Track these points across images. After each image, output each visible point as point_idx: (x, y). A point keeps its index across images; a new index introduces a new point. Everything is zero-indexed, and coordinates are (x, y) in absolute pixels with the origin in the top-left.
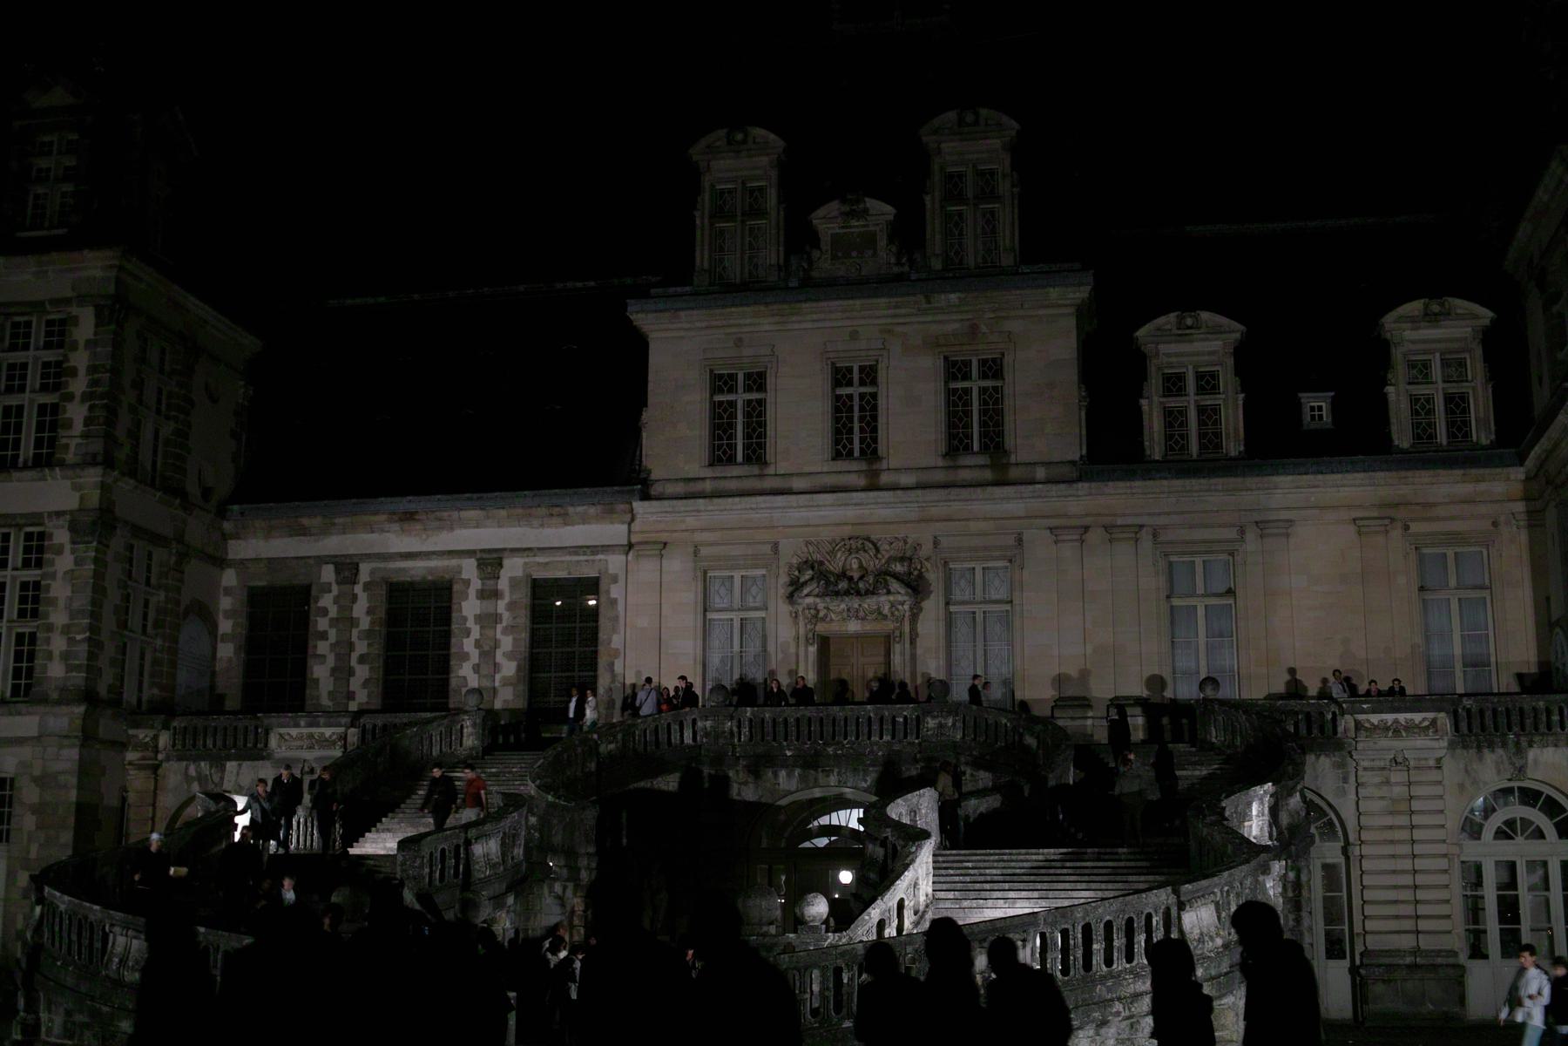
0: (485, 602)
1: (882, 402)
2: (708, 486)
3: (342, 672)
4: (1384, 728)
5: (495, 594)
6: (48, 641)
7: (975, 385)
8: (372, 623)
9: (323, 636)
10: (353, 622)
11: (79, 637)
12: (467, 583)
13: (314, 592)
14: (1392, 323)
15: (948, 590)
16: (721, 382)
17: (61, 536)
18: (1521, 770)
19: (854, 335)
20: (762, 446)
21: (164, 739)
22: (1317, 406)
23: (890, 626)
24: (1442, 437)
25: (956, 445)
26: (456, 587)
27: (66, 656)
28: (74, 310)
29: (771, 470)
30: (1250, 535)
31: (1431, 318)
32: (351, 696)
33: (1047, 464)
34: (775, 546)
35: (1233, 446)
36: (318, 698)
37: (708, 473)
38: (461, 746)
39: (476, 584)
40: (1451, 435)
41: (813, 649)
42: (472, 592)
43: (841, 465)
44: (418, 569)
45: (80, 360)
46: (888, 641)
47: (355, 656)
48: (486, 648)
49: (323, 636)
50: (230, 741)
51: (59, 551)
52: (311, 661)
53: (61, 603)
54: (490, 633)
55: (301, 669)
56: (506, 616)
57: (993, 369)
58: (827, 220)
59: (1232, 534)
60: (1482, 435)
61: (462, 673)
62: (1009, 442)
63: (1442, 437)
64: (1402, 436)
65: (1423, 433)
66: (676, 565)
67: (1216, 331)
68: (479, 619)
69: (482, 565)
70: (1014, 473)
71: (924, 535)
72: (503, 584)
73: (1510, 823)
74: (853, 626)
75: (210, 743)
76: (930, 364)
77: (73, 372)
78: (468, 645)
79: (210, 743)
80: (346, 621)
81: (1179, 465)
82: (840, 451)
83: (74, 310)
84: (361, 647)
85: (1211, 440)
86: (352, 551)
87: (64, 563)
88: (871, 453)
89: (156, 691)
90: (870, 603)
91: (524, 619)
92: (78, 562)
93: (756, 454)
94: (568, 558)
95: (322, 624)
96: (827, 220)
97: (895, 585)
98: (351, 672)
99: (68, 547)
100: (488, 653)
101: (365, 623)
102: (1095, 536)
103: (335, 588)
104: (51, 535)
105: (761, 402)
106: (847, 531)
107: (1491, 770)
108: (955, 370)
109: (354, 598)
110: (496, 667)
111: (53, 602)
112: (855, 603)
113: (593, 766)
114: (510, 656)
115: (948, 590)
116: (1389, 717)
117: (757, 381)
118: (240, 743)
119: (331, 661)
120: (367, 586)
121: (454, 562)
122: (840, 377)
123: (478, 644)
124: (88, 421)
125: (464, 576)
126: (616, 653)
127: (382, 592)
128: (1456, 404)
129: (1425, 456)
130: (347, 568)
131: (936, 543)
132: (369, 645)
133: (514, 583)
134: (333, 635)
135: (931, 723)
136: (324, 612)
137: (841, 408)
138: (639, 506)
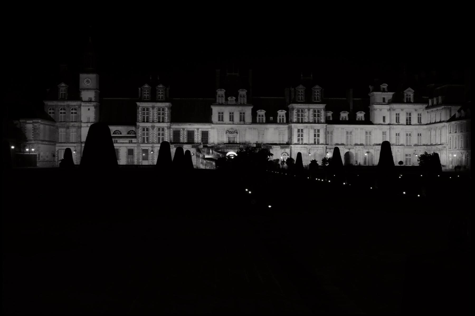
1: (234, 116)
2: (218, 123)
4: (275, 147)
7: (242, 115)
9: (181, 135)
10: (184, 134)
12: (196, 131)
13: (180, 131)
14: (278, 112)
15: (240, 132)
16: (219, 113)
17: (166, 129)
18: (285, 151)
19: (232, 110)
20: (223, 119)
21: (173, 146)
22: (271, 118)
23: (235, 136)
24: (282, 122)
25: (241, 120)
26: (195, 131)
27: (167, 139)
28: (165, 108)
29: (224, 122)
30: (265, 129)
31: (281, 111)
32: (184, 141)
33: (249, 122)
34: (224, 129)
35: (264, 122)
37: (218, 122)
39: (196, 131)
40: (282, 122)
41: (228, 138)
43: (230, 122)
44: (191, 130)
45: (166, 113)
46: (234, 137)
49: (181, 135)
51: (166, 130)
57: (244, 113)
58: (229, 98)
59: (264, 129)
60: (285, 122)
62: (245, 120)
63: (282, 122)
64: (278, 122)
65: (280, 121)
66: (215, 130)
67: (264, 111)
68: (197, 134)
69: (197, 129)
70: (246, 123)
71: (237, 128)
72: (199, 131)
73: (284, 155)
74: (232, 136)
76: (239, 113)
77: (166, 114)
80: (184, 134)
81: (260, 123)
82: (230, 120)
83: (165, 108)
84: (185, 137)
85: (262, 121)
87: (166, 131)
88: (233, 121)
90: (233, 134)
91: (201, 134)
92: (168, 131)
93: (222, 120)
95: (181, 134)
96: (229, 98)
97: (235, 133)
98: (184, 139)
100: (198, 137)
101: (186, 134)
102: (252, 129)
104: (165, 129)
105: (223, 115)
106: (231, 128)
107: (283, 151)
108: (241, 113)
109: (184, 132)
112: (232, 134)
114: (200, 138)
115: (240, 132)
116: (276, 147)
117: (222, 113)
119: (182, 138)
120: (186, 131)
122: (230, 113)
123: (197, 137)
124: (168, 118)
126: (210, 138)
127: (187, 131)
128: (283, 119)
129: (280, 123)
130: (184, 129)
131: (239, 129)
133: (200, 131)
134: (182, 135)
135: (241, 146)
136: (181, 133)
137: (230, 116)
138: (212, 125)
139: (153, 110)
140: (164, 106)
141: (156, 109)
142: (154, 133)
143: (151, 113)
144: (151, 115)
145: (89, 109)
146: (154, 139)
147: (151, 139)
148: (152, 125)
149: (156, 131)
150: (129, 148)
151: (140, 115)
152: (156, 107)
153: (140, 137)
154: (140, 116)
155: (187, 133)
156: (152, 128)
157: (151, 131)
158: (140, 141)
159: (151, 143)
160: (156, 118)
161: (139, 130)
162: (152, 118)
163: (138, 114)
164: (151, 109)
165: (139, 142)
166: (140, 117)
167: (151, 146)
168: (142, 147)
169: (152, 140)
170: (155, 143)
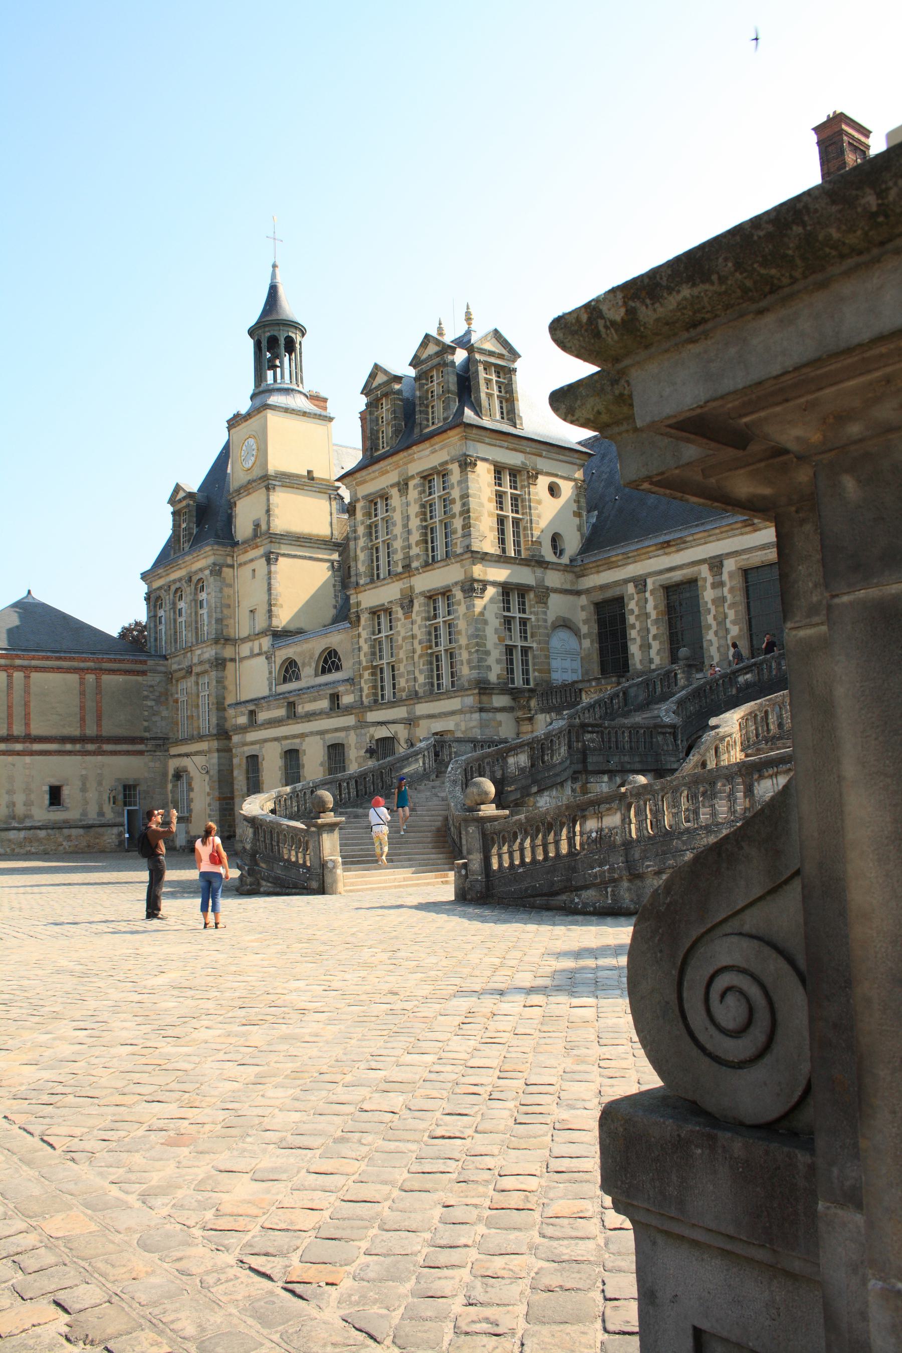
0: (716, 590)
3: (646, 647)
5: (721, 584)
6: (460, 654)
8: (657, 614)
10: (647, 615)
11: (473, 650)
12: (705, 579)
13: (626, 601)
17: (458, 594)
26: (700, 583)
28: (450, 467)
32: (651, 661)
36: (635, 665)
38: (676, 685)
39: (710, 580)
42: (708, 585)
47: (651, 636)
48: (720, 620)
50: (564, 699)
51: (459, 604)
52: (629, 643)
53: (464, 632)
54: (721, 609)
55: (625, 648)
56: (729, 597)
61: (709, 638)
69: (711, 569)
72: (725, 577)
75: (554, 701)
77: (453, 501)
78: (710, 619)
79: (554, 701)
83: (450, 467)
84: (653, 631)
86: (641, 572)
87: (461, 609)
89: (536, 674)
91: (740, 597)
94: (759, 553)
95: (631, 619)
99: (463, 601)
100: (721, 621)
101: (654, 615)
103: (636, 596)
109: (646, 600)
110: (727, 631)
111: (459, 633)
113: (734, 691)
114: (734, 623)
118: (569, 699)
121: (696, 568)
123: (715, 618)
125: (703, 575)
127: (661, 593)
130: (640, 582)
132: (658, 628)
133: (731, 575)
136: (632, 611)
139: (404, 498)
140: (447, 458)
141: (415, 487)
142: (413, 637)
143: (397, 517)
144: (398, 530)
145: (254, 570)
146: (417, 674)
147: (402, 676)
148: (401, 590)
149: (419, 619)
150: (332, 738)
151: (361, 542)
152: (413, 477)
153: (365, 668)
154: (362, 550)
155: (662, 607)
156: (403, 608)
157: (401, 628)
158: (367, 697)
159: (404, 695)
160: (417, 545)
161: (361, 629)
162: (403, 548)
163: (352, 544)
164: (394, 492)
165: (361, 696)
166: (362, 556)
167: (405, 715)
168: (372, 730)
169: (407, 681)
170: (421, 692)
